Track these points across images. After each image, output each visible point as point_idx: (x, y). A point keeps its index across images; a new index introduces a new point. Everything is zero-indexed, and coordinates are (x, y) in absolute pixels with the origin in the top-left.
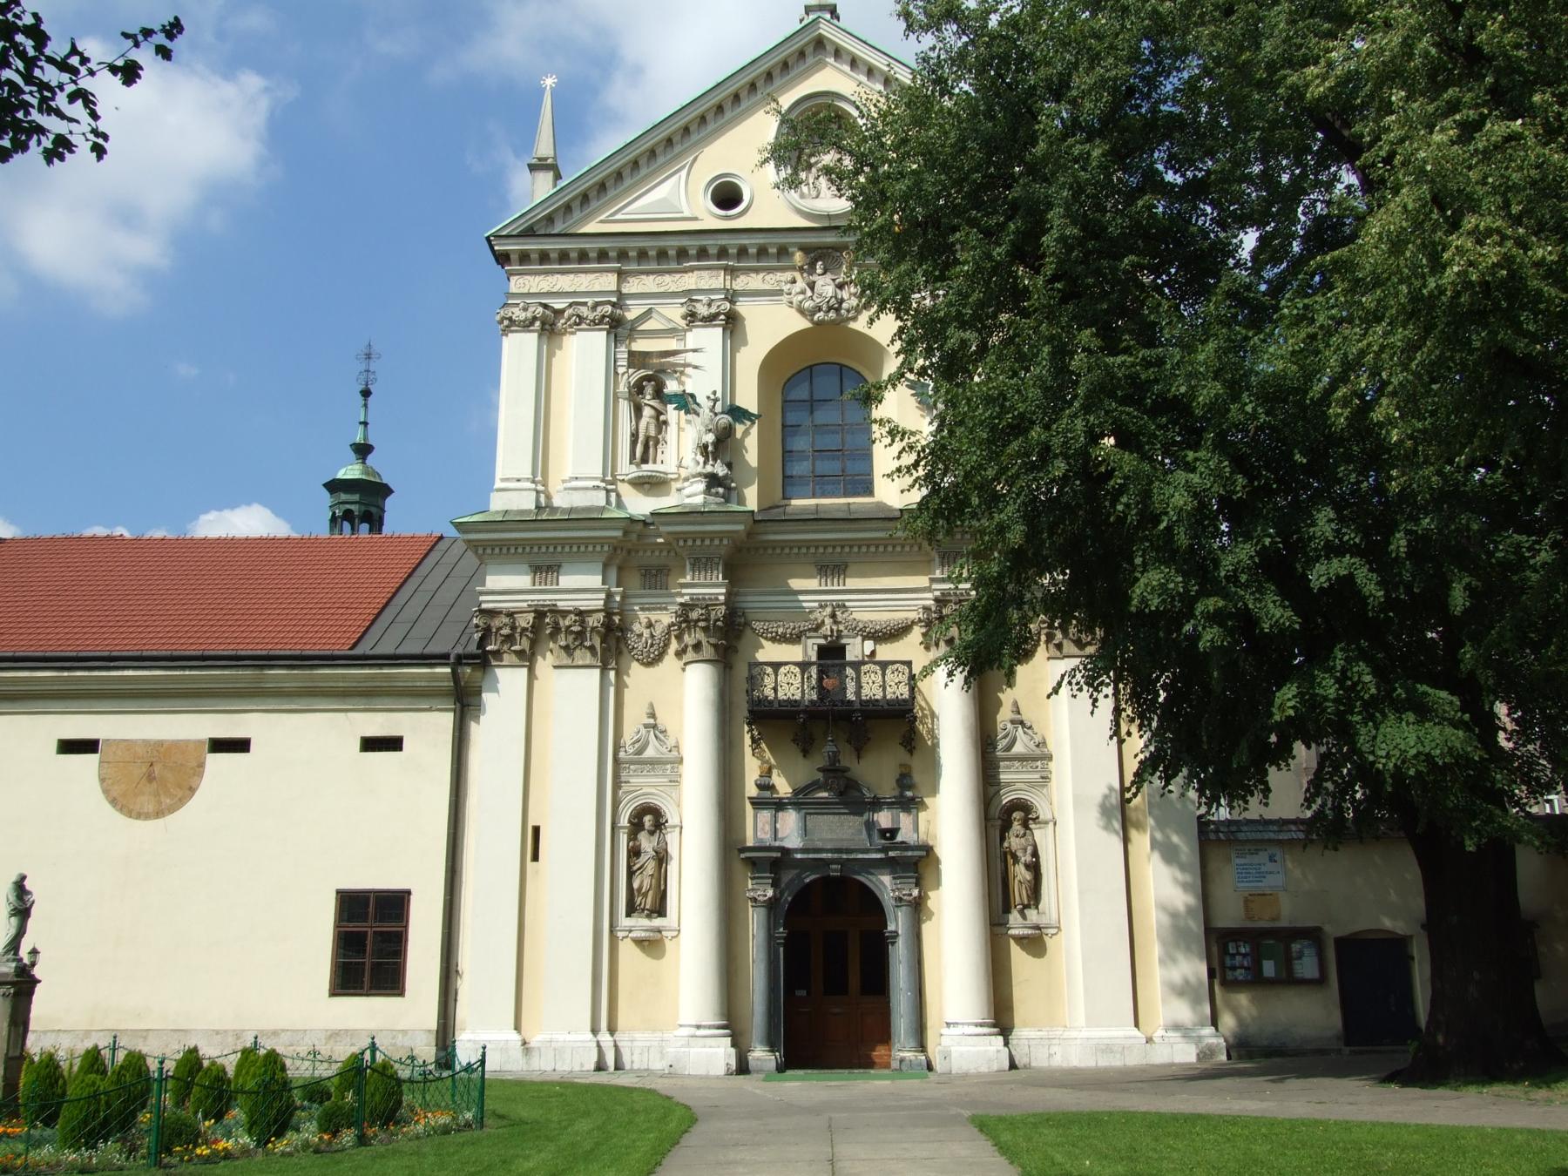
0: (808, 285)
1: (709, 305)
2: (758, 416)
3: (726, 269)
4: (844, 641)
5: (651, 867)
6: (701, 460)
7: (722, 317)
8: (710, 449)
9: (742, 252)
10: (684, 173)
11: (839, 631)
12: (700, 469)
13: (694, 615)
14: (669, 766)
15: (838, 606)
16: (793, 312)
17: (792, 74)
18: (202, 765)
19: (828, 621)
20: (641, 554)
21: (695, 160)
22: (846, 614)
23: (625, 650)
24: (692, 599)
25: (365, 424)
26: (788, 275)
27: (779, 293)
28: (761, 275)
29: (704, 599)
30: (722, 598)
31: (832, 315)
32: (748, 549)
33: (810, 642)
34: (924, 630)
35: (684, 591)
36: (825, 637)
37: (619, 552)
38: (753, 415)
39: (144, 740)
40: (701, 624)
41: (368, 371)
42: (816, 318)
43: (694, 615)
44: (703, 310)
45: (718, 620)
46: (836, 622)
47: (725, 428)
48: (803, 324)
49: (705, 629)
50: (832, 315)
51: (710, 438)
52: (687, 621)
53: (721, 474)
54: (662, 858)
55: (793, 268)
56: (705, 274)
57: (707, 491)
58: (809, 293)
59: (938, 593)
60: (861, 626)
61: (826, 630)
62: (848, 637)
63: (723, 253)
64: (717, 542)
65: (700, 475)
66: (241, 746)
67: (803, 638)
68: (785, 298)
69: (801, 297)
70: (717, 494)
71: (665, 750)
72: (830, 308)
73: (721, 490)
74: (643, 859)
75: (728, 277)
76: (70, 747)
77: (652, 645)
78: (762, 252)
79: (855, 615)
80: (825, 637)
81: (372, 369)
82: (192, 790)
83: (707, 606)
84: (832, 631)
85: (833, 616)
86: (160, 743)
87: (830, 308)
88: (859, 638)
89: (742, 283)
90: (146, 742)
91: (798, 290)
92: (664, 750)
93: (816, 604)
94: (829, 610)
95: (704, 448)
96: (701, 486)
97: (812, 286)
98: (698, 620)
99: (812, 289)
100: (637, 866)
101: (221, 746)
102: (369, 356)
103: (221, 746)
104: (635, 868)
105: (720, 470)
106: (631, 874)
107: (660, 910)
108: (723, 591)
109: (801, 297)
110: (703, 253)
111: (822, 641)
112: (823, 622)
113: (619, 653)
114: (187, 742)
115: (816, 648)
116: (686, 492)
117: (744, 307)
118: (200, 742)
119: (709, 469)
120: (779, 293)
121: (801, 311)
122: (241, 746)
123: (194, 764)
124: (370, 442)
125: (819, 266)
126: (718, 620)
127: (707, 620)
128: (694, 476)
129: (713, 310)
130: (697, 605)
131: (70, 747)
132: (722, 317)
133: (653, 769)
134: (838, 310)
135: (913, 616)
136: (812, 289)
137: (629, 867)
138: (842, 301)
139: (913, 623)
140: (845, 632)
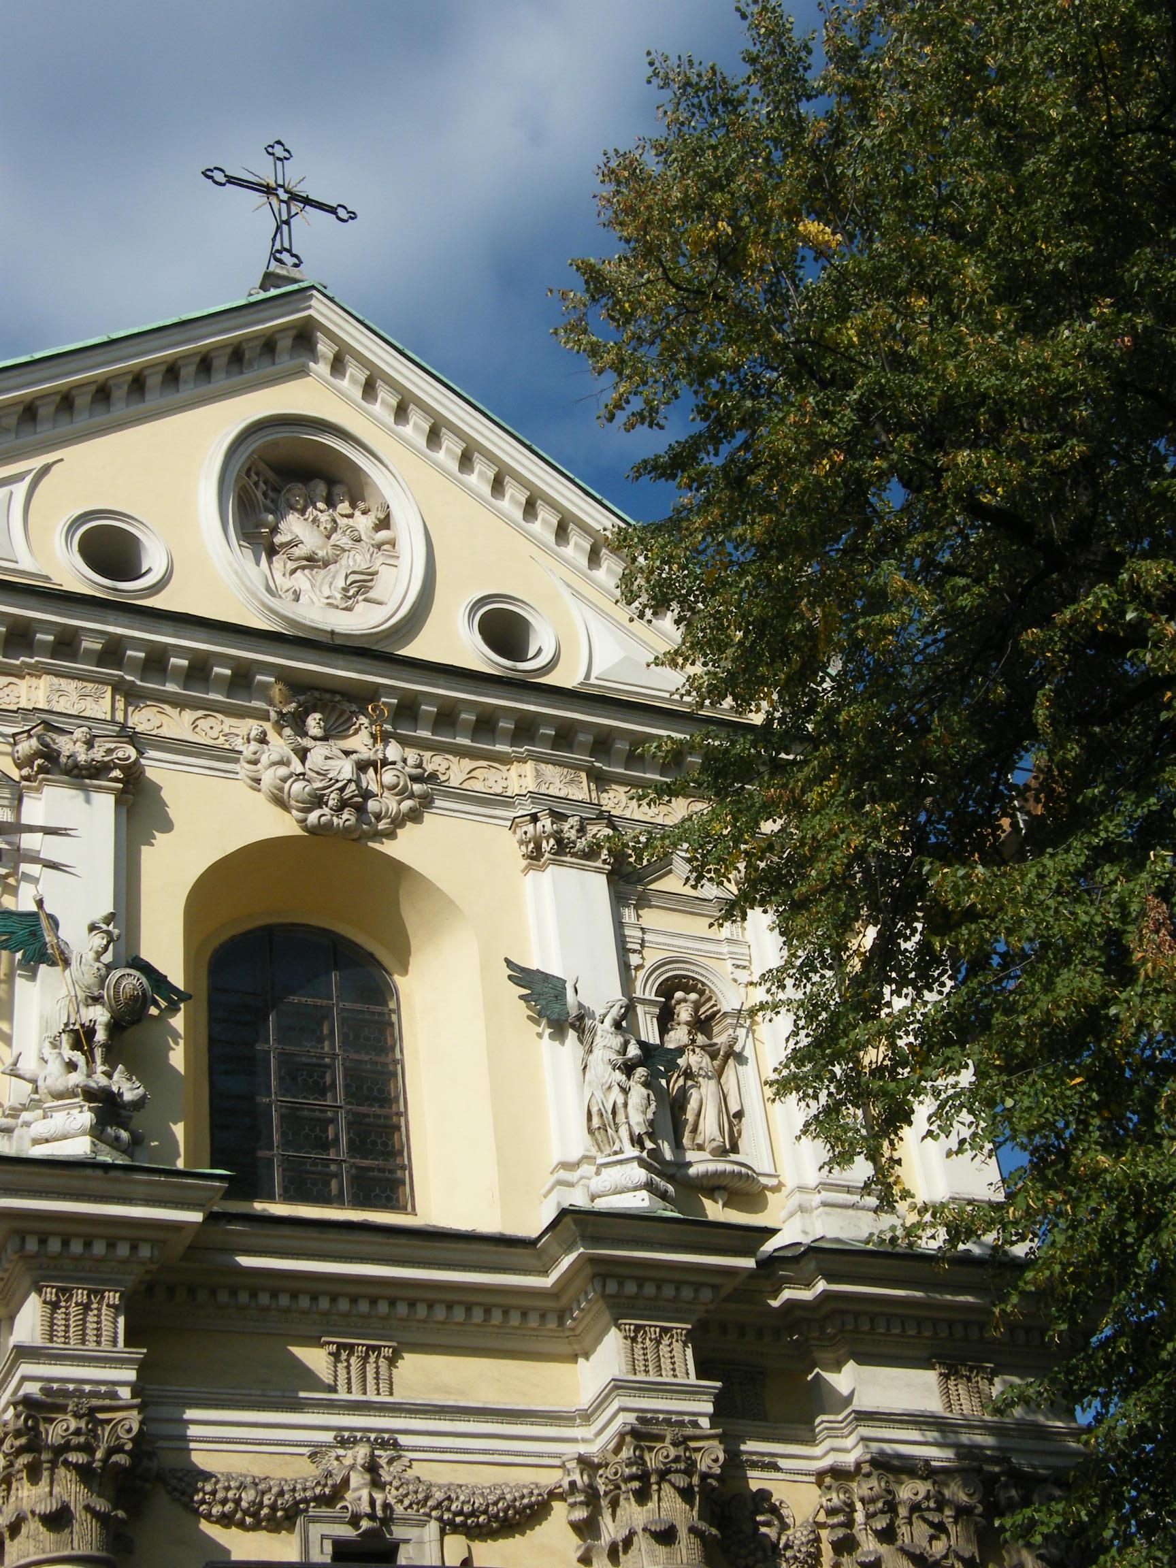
0: (295, 751)
1: (90, 744)
2: (184, 997)
3: (119, 687)
4: (398, 1532)
6: (78, 1057)
7: (116, 773)
8: (101, 1036)
9: (156, 662)
10: (21, 489)
11: (387, 1506)
12: (77, 1078)
13: (55, 1433)
15: (384, 1445)
16: (261, 801)
17: (248, 376)
19: (356, 1479)
21: (46, 469)
22: (397, 1467)
24: (46, 1391)
26: (253, 726)
27: (231, 756)
28: (189, 715)
29: (80, 1394)
30: (125, 1393)
31: (348, 816)
32: (171, 1290)
33: (316, 1530)
34: (581, 1514)
35: (26, 1369)
36: (355, 1521)
38: (175, 990)
40: (73, 1457)
42: (313, 817)
43: (55, 1433)
44: (70, 746)
45: (119, 1449)
46: (377, 1483)
47: (134, 998)
48: (284, 825)
49: (85, 1473)
50: (348, 816)
51: (99, 1015)
52: (34, 1445)
53: (128, 1096)
55: (265, 717)
56: (71, 686)
57: (97, 1132)
58: (297, 766)
59: (631, 1418)
60: (439, 1495)
61: (359, 1495)
62: (405, 1521)
63: (112, 652)
64: (123, 1250)
65: (69, 1093)
67: (300, 1521)
68: (243, 769)
69: (283, 771)
70: (115, 1143)
72: (343, 805)
73: (124, 1135)
75: (120, 704)
78: (199, 671)
79: (418, 1470)
80: (355, 1521)
83: (93, 1410)
84: (372, 1502)
85: (372, 1468)
87: (343, 805)
88: (433, 1527)
89: (144, 719)
91: (275, 757)
93: (328, 1437)
94: (362, 1452)
95: (82, 1038)
96: (85, 1117)
97: (303, 754)
98: (66, 1447)
99: (303, 760)
105: (128, 1089)
108: (130, 1375)
109: (283, 771)
110: (66, 644)
111: (346, 1532)
112: (346, 1481)
115: (328, 1547)
116: (41, 1127)
117: (157, 769)
119: (100, 1080)
120: (231, 756)
121: (280, 801)
125: (314, 723)
126: (119, 1449)
127: (88, 1449)
128: (59, 1096)
129: (98, 754)
130: (62, 1409)
132: (116, 773)
134: (360, 809)
135: (550, 1478)
136: (303, 760)
138: (367, 795)
139: (553, 1495)
140: (399, 1509)
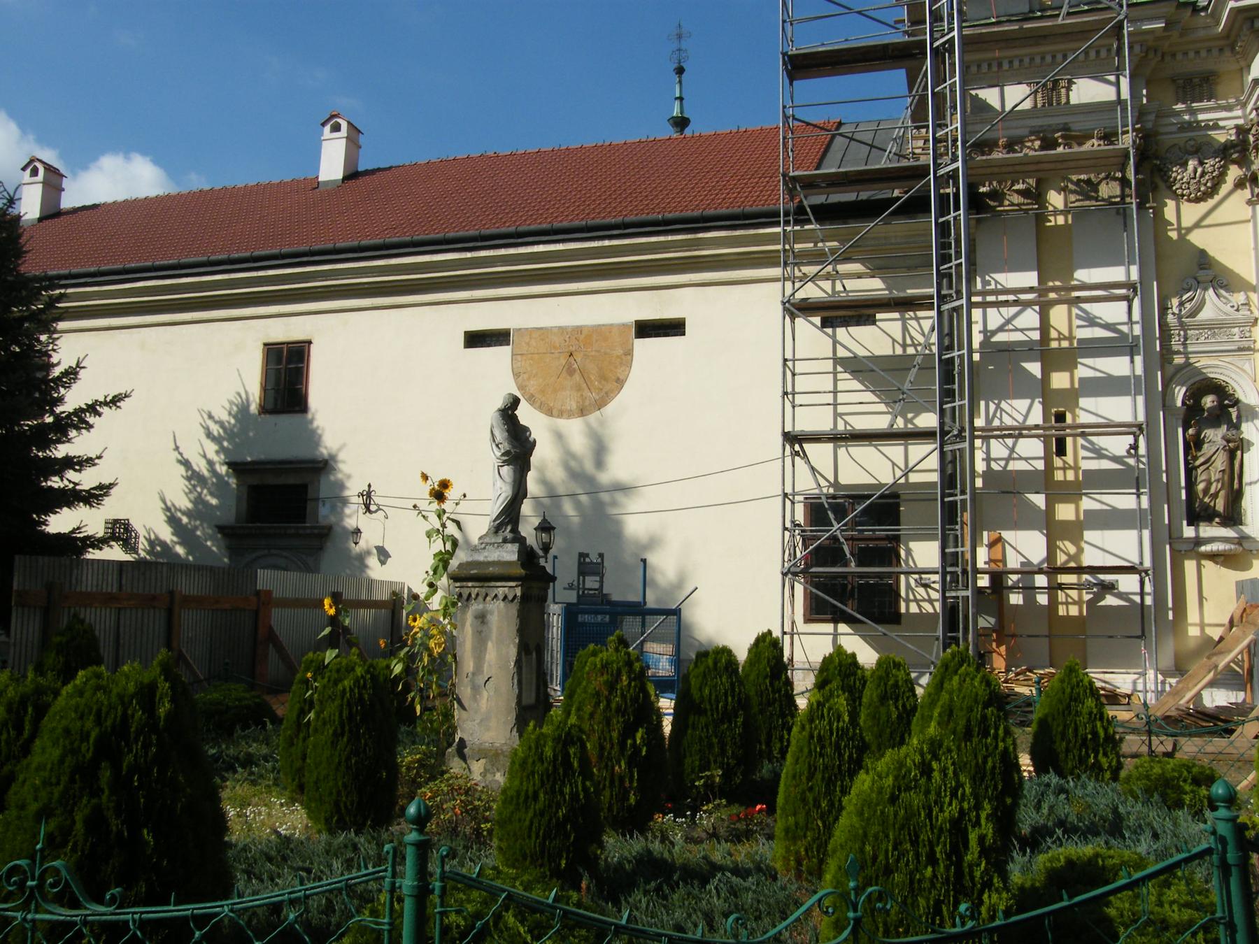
5: (1220, 462)
14: (1236, 330)
18: (629, 353)
20: (1179, 57)
23: (1162, 185)
25: (681, 99)
37: (1151, 55)
39: (560, 328)
41: (679, 50)
54: (1235, 449)
66: (674, 328)
71: (1227, 308)
74: (1207, 450)
76: (475, 339)
77: (1202, 175)
81: (683, 47)
82: (620, 383)
86: (579, 329)
90: (562, 329)
92: (1227, 308)
100: (1201, 460)
101: (647, 329)
102: (680, 37)
103: (647, 329)
104: (1198, 463)
106: (1190, 471)
107: (1233, 517)
113: (1155, 188)
114: (612, 325)
118: (624, 325)
122: (674, 328)
123: (620, 352)
124: (685, 116)
131: (475, 339)
133: (1214, 335)
137: (1187, 463)
